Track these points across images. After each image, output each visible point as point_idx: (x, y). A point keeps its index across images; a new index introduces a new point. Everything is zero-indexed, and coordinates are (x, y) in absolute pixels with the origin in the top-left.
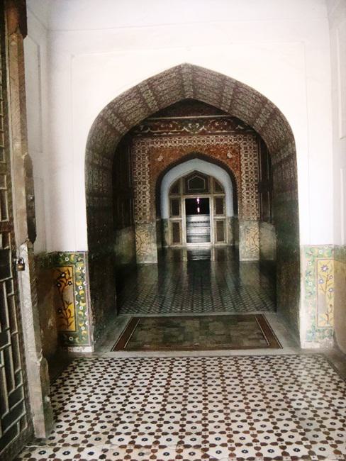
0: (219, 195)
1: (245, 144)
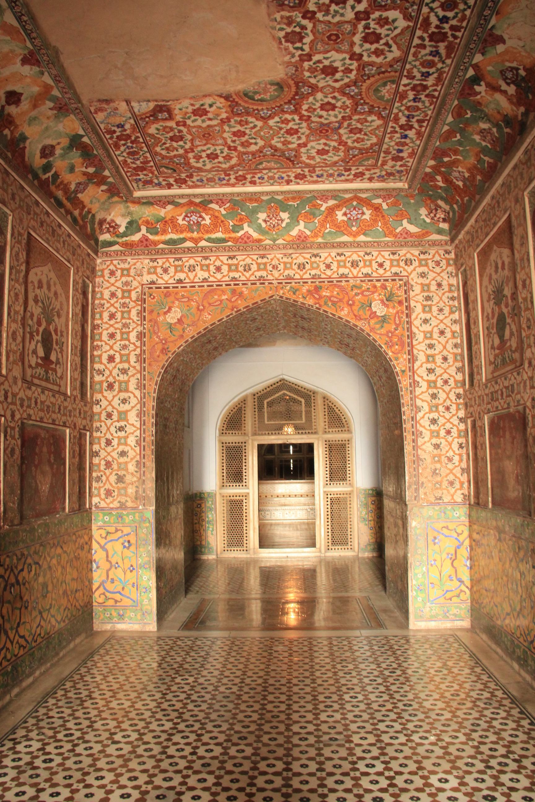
0: (336, 436)
1: (423, 275)
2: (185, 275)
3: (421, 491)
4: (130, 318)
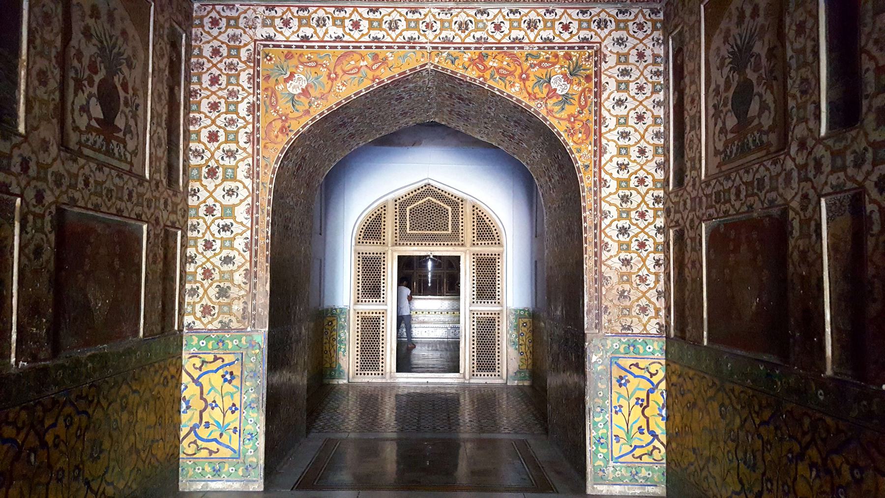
2: (312, 30)
3: (605, 318)
4: (238, 85)
